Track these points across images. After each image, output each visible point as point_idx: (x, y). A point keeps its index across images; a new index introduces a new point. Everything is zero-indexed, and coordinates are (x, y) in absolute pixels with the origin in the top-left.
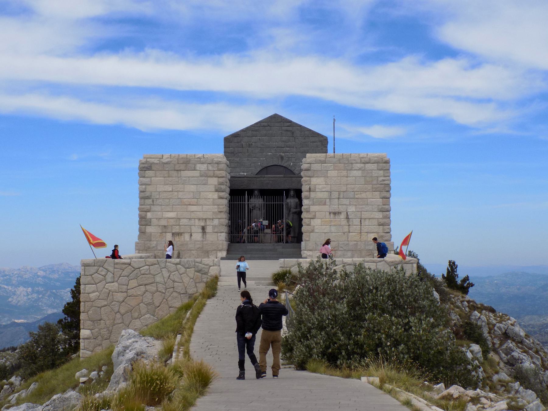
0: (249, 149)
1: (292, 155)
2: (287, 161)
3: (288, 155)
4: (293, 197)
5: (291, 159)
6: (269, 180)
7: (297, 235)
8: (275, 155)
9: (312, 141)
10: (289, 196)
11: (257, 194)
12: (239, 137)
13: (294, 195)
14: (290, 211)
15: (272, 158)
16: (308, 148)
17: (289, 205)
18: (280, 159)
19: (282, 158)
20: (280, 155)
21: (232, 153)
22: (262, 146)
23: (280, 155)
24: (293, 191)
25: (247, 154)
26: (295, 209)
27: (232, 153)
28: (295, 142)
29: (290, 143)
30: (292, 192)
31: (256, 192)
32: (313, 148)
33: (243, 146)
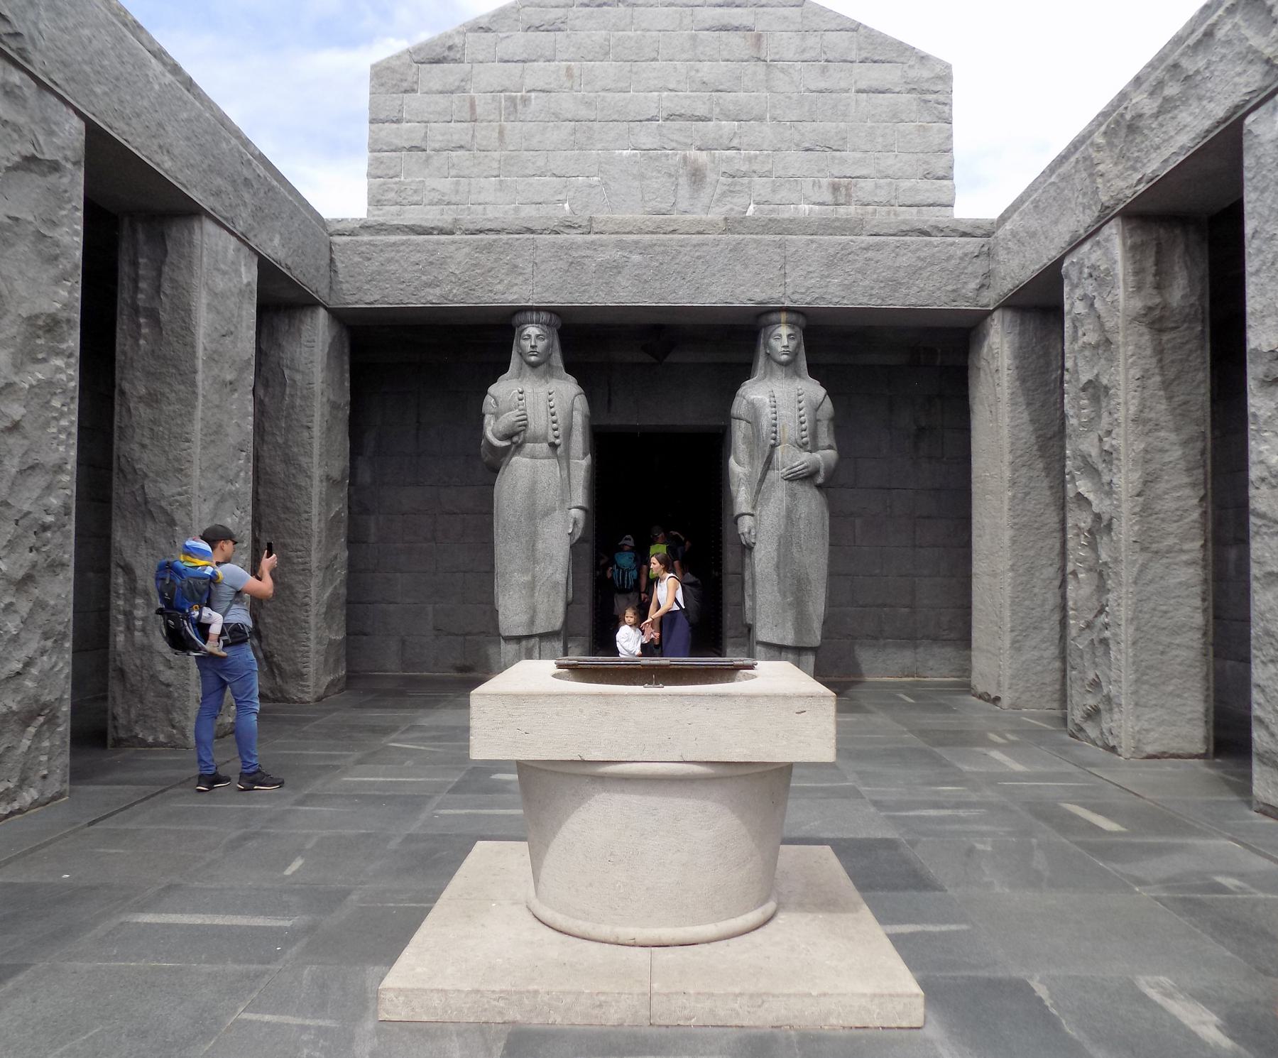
0: (508, 125)
1: (750, 159)
2: (724, 194)
3: (729, 160)
4: (789, 366)
5: (746, 180)
6: (620, 245)
7: (815, 639)
8: (657, 159)
9: (863, 85)
10: (761, 361)
11: (541, 345)
12: (455, 61)
13: (794, 355)
14: (769, 463)
15: (642, 177)
16: (842, 125)
17: (765, 423)
18: (683, 181)
19: (697, 176)
20: (685, 158)
21: (411, 149)
22: (583, 112)
23: (685, 158)
24: (791, 324)
25: (496, 155)
26: (803, 446)
27: (411, 149)
28: (769, 89)
29: (741, 95)
30: (784, 331)
31: (532, 330)
32: (869, 124)
33: (479, 110)
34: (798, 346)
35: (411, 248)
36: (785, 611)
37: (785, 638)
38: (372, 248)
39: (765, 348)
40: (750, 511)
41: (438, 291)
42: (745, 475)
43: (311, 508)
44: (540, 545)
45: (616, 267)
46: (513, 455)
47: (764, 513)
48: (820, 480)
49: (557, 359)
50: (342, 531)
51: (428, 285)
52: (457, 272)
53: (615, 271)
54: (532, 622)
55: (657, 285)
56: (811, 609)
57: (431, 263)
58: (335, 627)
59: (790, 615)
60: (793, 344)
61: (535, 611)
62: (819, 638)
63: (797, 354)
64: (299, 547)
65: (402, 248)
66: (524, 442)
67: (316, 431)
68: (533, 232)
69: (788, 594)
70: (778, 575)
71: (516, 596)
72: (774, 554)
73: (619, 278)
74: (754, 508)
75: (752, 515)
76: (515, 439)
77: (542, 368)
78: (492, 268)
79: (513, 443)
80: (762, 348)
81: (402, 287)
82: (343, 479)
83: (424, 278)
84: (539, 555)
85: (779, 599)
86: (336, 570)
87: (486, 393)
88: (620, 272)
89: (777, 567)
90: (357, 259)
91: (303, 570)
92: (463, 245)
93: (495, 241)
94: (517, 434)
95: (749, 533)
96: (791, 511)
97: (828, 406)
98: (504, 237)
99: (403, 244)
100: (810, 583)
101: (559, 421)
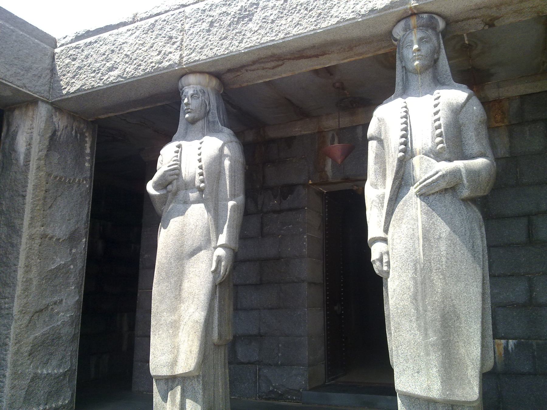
34: (436, 51)
35: (101, 43)
36: (428, 354)
37: (429, 388)
38: (77, 50)
39: (402, 62)
40: (382, 235)
41: (116, 73)
42: (378, 197)
43: (18, 261)
44: (186, 285)
45: (247, 16)
46: (171, 202)
47: (395, 237)
48: (466, 193)
49: (214, 115)
50: (72, 280)
51: (111, 69)
52: (129, 53)
53: (247, 19)
54: (174, 363)
55: (283, 22)
56: (462, 351)
57: (113, 51)
58: (54, 363)
59: (435, 359)
60: (426, 48)
61: (178, 351)
62: (476, 390)
63: (436, 61)
64: (7, 295)
65: (95, 45)
66: (178, 190)
67: (29, 198)
68: (184, 6)
69: (430, 332)
70: (417, 309)
71: (164, 335)
72: (410, 283)
73: (251, 25)
74: (386, 231)
75: (385, 240)
76: (170, 187)
77: (200, 124)
78: (154, 43)
79: (168, 192)
80: (398, 63)
81: (93, 75)
82: (73, 238)
83: (108, 64)
84: (184, 294)
85: (419, 338)
86: (58, 313)
87: (160, 154)
88: (250, 20)
89: (415, 298)
90: (67, 61)
91: (8, 314)
92: (134, 31)
93: (156, 21)
94: (170, 183)
95: (381, 260)
96: (428, 231)
97: (476, 107)
98: (163, 17)
99: (96, 42)
100: (458, 318)
101: (204, 167)
